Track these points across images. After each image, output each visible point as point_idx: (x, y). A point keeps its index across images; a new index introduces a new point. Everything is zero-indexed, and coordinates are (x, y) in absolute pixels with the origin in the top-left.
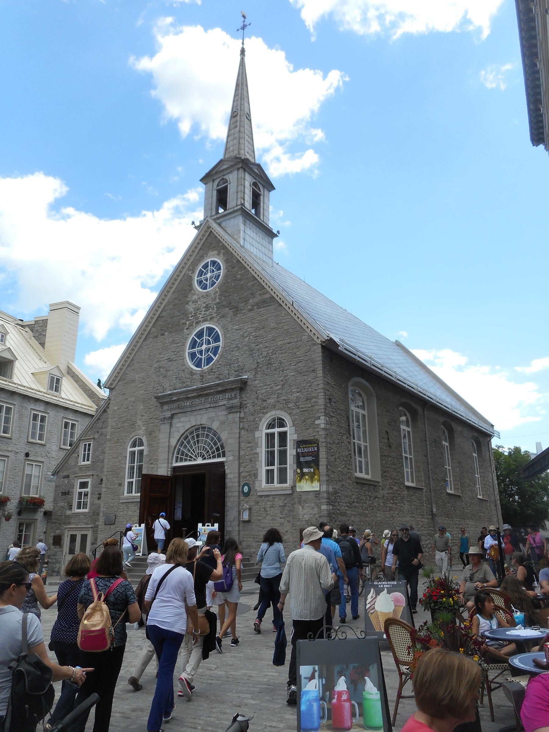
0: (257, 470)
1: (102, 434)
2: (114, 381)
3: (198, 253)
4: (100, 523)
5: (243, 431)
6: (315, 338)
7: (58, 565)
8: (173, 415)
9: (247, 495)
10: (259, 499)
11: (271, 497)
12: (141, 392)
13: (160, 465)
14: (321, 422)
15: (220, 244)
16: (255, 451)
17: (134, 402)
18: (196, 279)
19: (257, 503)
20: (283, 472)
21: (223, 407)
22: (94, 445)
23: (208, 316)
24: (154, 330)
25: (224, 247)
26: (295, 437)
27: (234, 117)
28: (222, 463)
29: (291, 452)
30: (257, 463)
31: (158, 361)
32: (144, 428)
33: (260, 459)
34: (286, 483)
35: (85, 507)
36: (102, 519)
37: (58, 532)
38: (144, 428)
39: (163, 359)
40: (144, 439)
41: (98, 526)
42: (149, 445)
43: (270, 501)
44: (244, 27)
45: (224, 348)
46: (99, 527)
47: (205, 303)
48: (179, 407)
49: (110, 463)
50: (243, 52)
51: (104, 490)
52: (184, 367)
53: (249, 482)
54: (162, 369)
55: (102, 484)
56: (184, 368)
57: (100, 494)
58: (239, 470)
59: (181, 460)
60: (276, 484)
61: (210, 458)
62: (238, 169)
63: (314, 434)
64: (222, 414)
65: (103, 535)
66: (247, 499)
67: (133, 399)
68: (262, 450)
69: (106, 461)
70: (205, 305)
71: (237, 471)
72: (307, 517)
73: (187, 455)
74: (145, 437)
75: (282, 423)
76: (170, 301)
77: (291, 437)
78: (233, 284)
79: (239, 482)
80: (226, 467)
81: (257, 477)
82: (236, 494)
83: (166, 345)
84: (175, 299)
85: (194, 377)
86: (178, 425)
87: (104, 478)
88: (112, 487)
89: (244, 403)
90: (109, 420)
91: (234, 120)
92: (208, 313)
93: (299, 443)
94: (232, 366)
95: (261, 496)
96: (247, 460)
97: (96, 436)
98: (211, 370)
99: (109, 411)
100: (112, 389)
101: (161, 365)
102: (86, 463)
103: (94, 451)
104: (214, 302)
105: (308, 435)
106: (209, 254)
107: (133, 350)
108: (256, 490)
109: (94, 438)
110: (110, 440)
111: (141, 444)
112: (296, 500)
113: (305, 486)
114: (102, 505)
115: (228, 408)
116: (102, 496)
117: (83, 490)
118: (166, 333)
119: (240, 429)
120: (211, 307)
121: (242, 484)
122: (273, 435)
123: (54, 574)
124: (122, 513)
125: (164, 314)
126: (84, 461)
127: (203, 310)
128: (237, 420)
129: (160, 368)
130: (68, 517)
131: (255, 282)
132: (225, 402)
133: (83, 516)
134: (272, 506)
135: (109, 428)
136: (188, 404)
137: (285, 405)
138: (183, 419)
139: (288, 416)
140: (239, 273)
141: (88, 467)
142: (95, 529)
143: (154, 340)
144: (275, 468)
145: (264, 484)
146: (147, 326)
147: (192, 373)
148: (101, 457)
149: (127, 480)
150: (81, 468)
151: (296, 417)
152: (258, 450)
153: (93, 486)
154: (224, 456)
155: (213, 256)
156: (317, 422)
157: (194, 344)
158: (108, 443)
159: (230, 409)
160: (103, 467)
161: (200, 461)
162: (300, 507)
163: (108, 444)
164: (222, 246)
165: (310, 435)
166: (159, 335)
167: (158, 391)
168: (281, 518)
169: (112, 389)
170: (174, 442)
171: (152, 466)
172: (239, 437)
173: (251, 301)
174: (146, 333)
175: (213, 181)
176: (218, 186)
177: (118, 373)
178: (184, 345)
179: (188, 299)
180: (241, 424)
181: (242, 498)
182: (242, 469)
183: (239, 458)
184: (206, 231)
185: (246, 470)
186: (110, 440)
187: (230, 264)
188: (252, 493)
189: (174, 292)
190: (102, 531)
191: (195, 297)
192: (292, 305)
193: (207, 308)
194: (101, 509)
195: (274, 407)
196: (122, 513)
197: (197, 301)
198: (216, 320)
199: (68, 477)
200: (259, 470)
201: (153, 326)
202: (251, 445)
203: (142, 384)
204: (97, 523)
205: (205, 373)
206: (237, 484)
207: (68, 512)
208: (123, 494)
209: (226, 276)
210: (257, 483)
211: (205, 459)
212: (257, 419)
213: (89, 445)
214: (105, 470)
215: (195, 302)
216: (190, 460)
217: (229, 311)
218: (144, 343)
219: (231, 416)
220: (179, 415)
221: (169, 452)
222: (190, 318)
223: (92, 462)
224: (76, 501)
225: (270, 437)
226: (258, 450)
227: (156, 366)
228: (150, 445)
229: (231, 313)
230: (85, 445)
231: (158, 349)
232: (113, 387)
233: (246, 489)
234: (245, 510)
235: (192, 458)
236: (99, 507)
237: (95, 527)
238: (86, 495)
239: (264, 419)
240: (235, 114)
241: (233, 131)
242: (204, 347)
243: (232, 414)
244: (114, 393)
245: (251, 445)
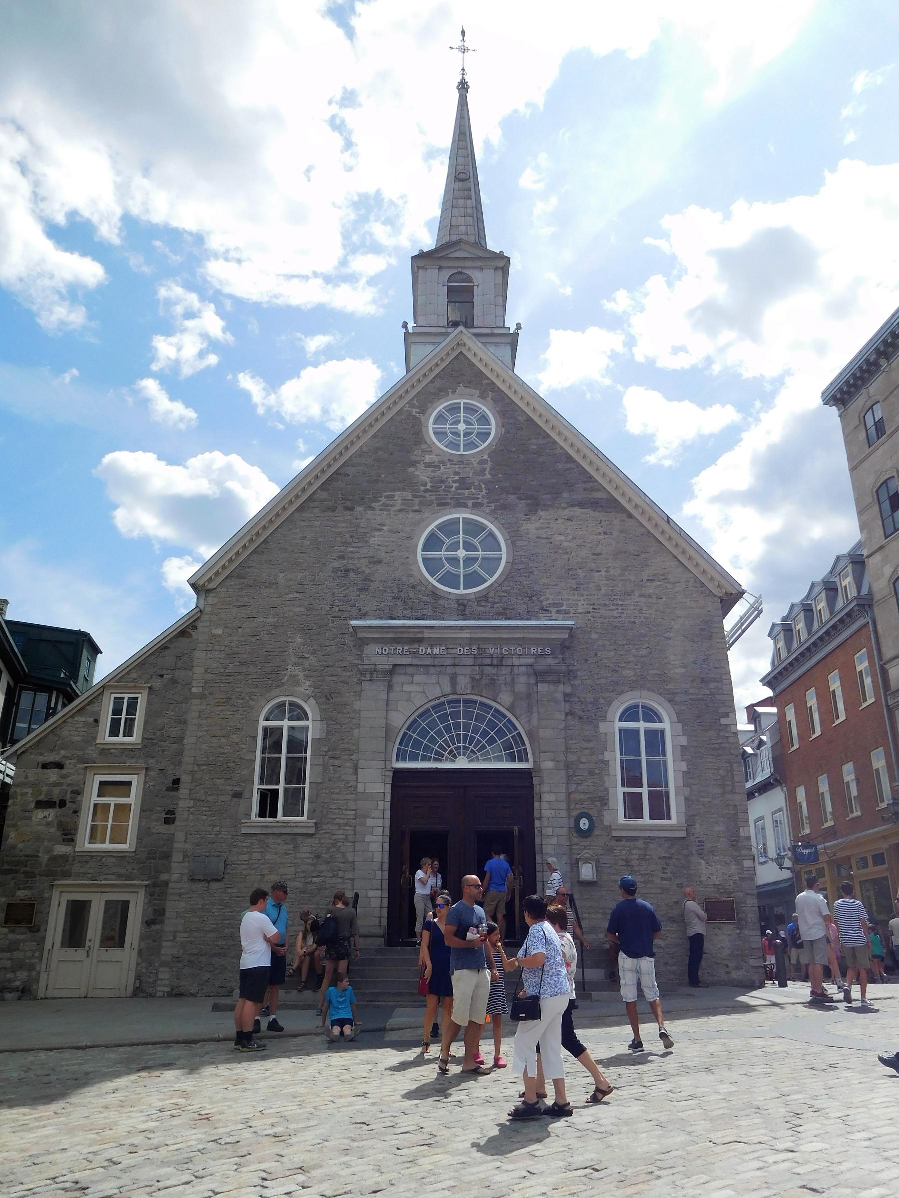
0: (607, 790)
1: (174, 681)
2: (217, 573)
3: (432, 382)
4: (175, 877)
5: (569, 717)
6: (710, 586)
7: (22, 975)
10: (614, 842)
11: (640, 844)
12: (296, 610)
13: (361, 763)
15: (485, 382)
16: (600, 757)
17: (275, 627)
19: (610, 850)
21: (523, 669)
22: (149, 703)
23: (468, 498)
24: (324, 495)
25: (492, 386)
26: (684, 741)
27: (463, 180)
30: (606, 778)
31: (343, 557)
32: (308, 683)
33: (612, 771)
34: (651, 818)
35: (118, 835)
36: (178, 870)
37: (21, 894)
38: (308, 683)
39: (356, 555)
41: (166, 883)
42: (326, 718)
43: (639, 849)
44: (464, 50)
45: (513, 563)
46: (171, 885)
47: (456, 473)
48: (416, 655)
49: (204, 747)
50: (463, 87)
52: (411, 580)
53: (591, 812)
54: (352, 574)
55: (177, 789)
56: (417, 585)
57: (171, 812)
58: (567, 788)
59: (414, 758)
60: (647, 820)
61: (489, 760)
62: (496, 268)
63: (719, 741)
65: (183, 905)
66: (585, 842)
67: (271, 620)
68: (615, 758)
69: (189, 740)
70: (457, 478)
71: (563, 788)
72: (715, 880)
73: (427, 749)
74: (312, 701)
75: (651, 715)
76: (364, 449)
78: (522, 457)
79: (569, 809)
80: (536, 781)
81: (606, 804)
82: (565, 831)
83: (361, 530)
84: (378, 449)
85: (441, 602)
86: (406, 688)
87: (185, 778)
88: (211, 798)
89: (571, 668)
90: (198, 654)
91: (459, 185)
92: (467, 492)
94: (534, 598)
95: (619, 839)
97: (158, 684)
98: (484, 598)
100: (208, 591)
101: (351, 566)
102: (121, 739)
103: (150, 714)
104: (480, 478)
106: (461, 389)
107: (271, 521)
108: (609, 828)
109: (150, 688)
110: (202, 697)
112: (694, 849)
114: (180, 836)
115: (536, 674)
116: (181, 815)
117: (112, 801)
118: (359, 509)
119: (567, 714)
120: (473, 483)
121: (575, 813)
122: (637, 732)
123: (8, 996)
124: (245, 857)
125: (351, 470)
126: (114, 732)
127: (455, 485)
128: (560, 696)
129: (347, 570)
130: (65, 858)
131: (572, 465)
132: (530, 661)
133: (114, 860)
134: (643, 858)
135: (199, 670)
136: (436, 651)
138: (417, 679)
139: (667, 704)
140: (534, 441)
141: (132, 750)
142: (157, 892)
143: (327, 514)
144: (644, 790)
145: (622, 819)
146: (310, 484)
147: (435, 595)
148: (175, 732)
149: (257, 786)
150: (106, 751)
151: (683, 708)
152: (607, 756)
153: (147, 794)
154: (523, 757)
155: (471, 396)
156: (723, 721)
157: (432, 542)
158: (194, 701)
160: (181, 753)
161: (462, 763)
162: (703, 862)
163: (196, 706)
164: (488, 385)
165: (712, 742)
166: (340, 508)
167: (345, 615)
168: (662, 879)
169: (208, 591)
170: (399, 719)
171: (337, 762)
172: (566, 728)
173: (566, 495)
174: (305, 497)
175: (440, 268)
176: (448, 281)
177: (231, 560)
179: (413, 458)
180: (568, 706)
181: (576, 840)
182: (573, 787)
183: (567, 766)
184: (453, 349)
185: (580, 788)
186: (202, 697)
187: (512, 421)
188: (596, 832)
189: (374, 436)
190: (180, 894)
191: (427, 458)
192: (668, 522)
193: (464, 483)
194: (176, 845)
195: (635, 685)
196: (245, 857)
197: (438, 467)
198: (488, 510)
199: (59, 766)
200: (611, 790)
201: (322, 487)
202: (590, 745)
203: (296, 595)
204: (164, 877)
205: (470, 600)
206: (564, 813)
207: (62, 849)
208: (249, 815)
210: (605, 813)
211: (472, 760)
212: (602, 701)
213: (133, 703)
214: (187, 759)
215: (434, 466)
216: (435, 760)
217: (518, 501)
218: (297, 515)
219: (543, 688)
220: (410, 670)
221: (387, 738)
222: (422, 493)
223: (144, 738)
224: (86, 821)
225: (629, 736)
226: (607, 756)
227: (336, 564)
228: (331, 718)
229: (522, 505)
230: (119, 701)
231: (340, 533)
232: (211, 586)
233: (584, 824)
234: (587, 861)
235: (442, 756)
236: (171, 839)
237: (155, 885)
238: (123, 810)
239: (615, 703)
240: (463, 176)
241: (461, 202)
242: (462, 553)
243: (546, 685)
244: (211, 600)
245: (590, 745)
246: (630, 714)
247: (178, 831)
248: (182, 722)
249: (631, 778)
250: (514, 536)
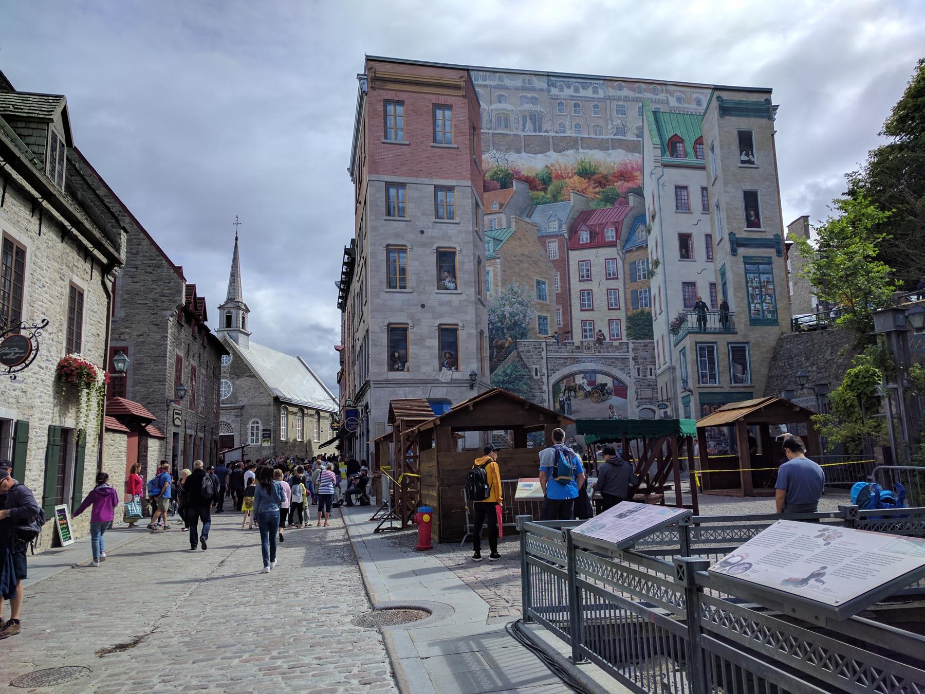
14: (272, 424)
20: (257, 439)
29: (260, 433)
44: (237, 224)
50: (237, 239)
64: (233, 418)
77: (261, 428)
93: (264, 430)
96: (243, 435)
105: (267, 428)
113: (265, 444)
137: (259, 417)
159: (237, 416)
195: (255, 417)
209: (233, 361)
225: (253, 427)
246: (253, 423)
249: (253, 434)
250: (234, 384)
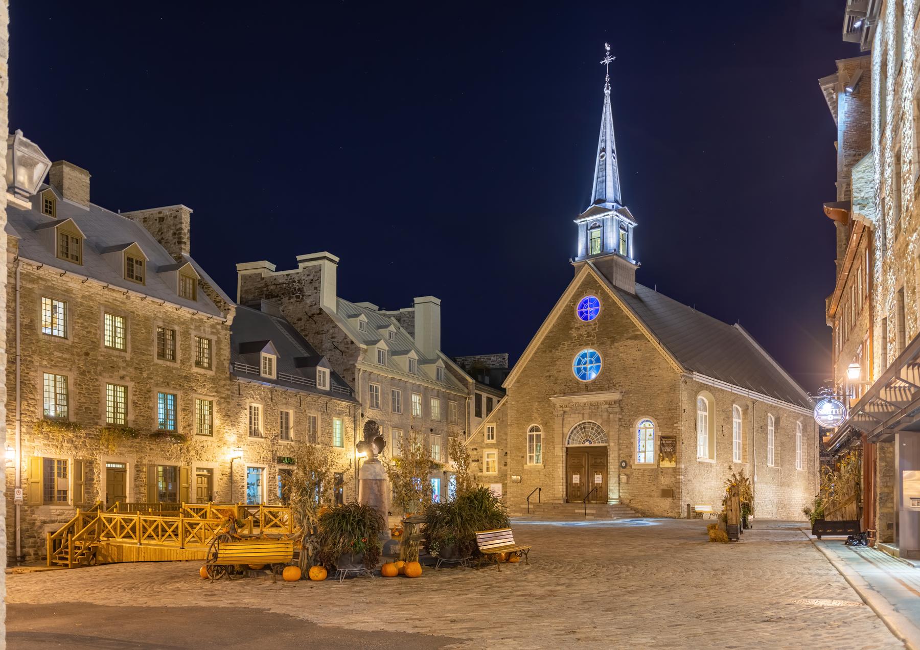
8: (565, 412)
9: (624, 468)
18: (577, 311)
28: (606, 447)
40: (540, 427)
51: (509, 460)
99: (508, 405)
111: (538, 430)
147: (578, 383)
149: (528, 455)
163: (509, 429)
178: (570, 361)
191: (576, 325)
215: (578, 329)
219: (611, 416)
233: (624, 464)
247: (508, 468)
248: (506, 434)
